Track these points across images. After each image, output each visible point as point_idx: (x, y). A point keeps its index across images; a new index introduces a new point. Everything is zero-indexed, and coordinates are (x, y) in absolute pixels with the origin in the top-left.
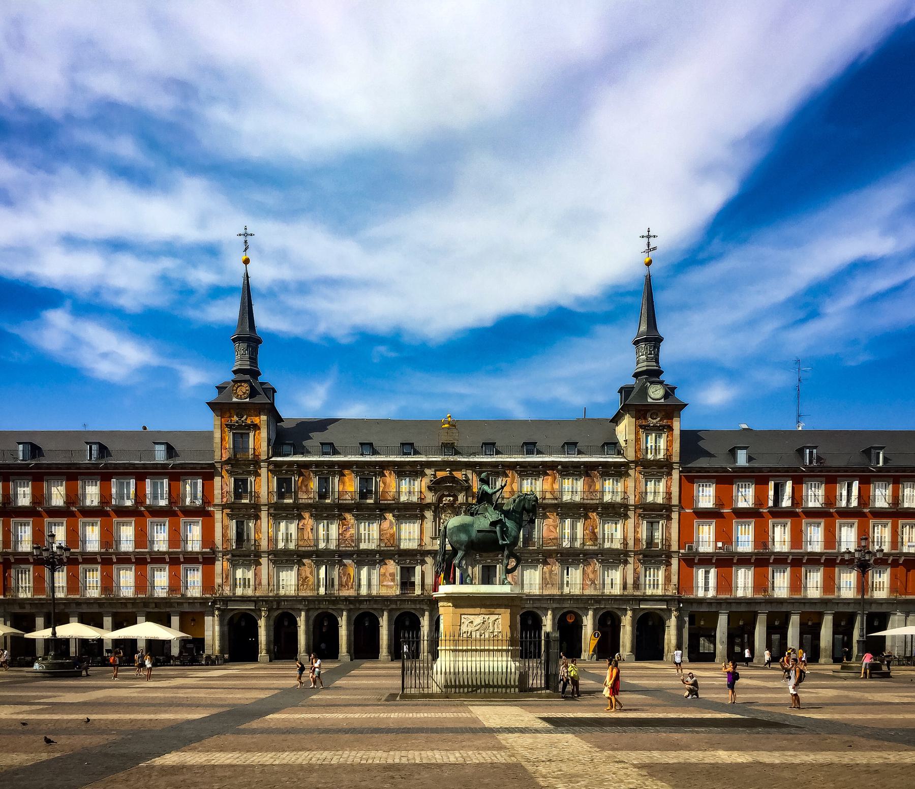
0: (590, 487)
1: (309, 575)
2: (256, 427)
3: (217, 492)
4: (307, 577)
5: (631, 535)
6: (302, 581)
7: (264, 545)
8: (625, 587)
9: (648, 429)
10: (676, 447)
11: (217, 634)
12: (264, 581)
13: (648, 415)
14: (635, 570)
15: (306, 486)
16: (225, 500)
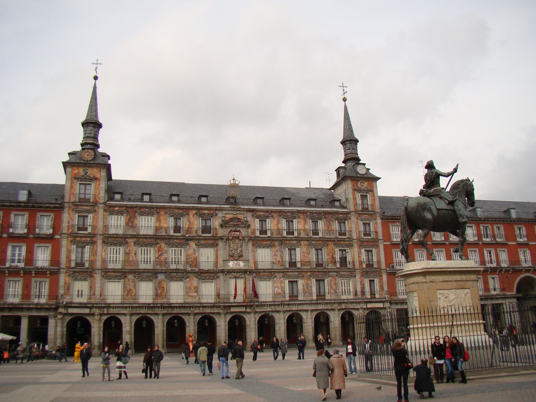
0: (329, 228)
1: (132, 288)
2: (96, 179)
3: (65, 225)
4: (130, 290)
5: (357, 259)
6: (127, 292)
7: (99, 265)
8: (356, 294)
9: (359, 191)
10: (377, 203)
11: (59, 333)
12: (98, 292)
13: (359, 183)
14: (361, 282)
15: (132, 222)
16: (70, 231)
